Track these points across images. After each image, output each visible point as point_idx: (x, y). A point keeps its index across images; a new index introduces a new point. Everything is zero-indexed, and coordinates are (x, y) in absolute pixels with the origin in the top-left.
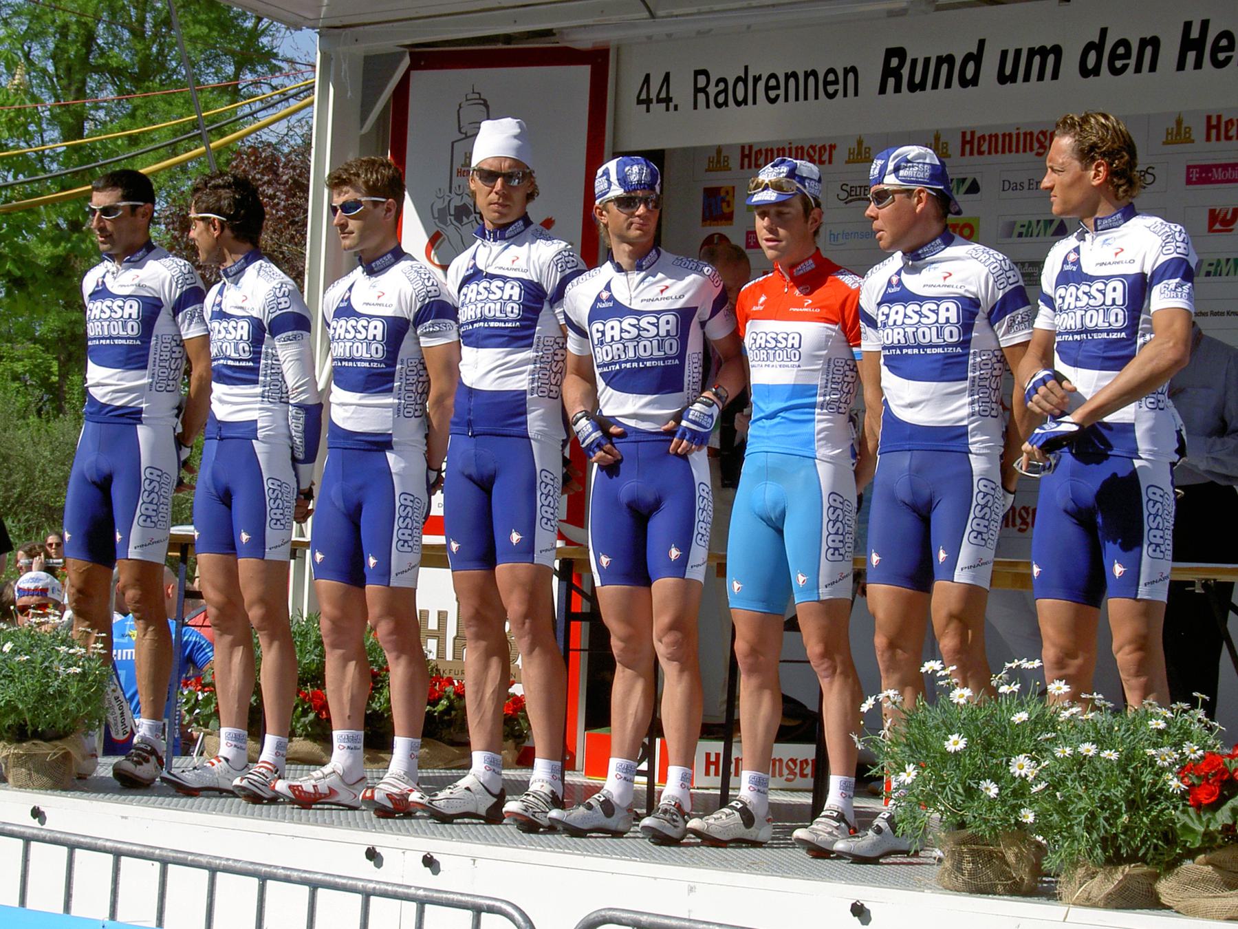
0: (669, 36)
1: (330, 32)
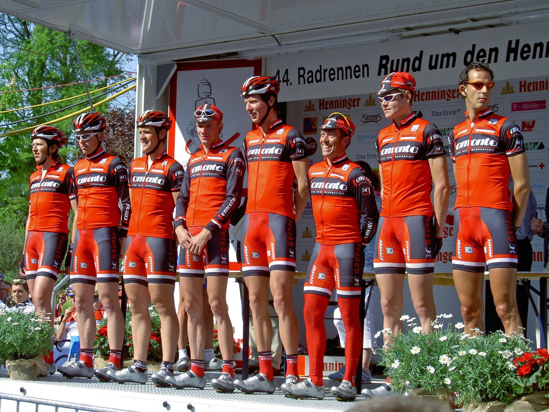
0: (287, 53)
1: (142, 55)
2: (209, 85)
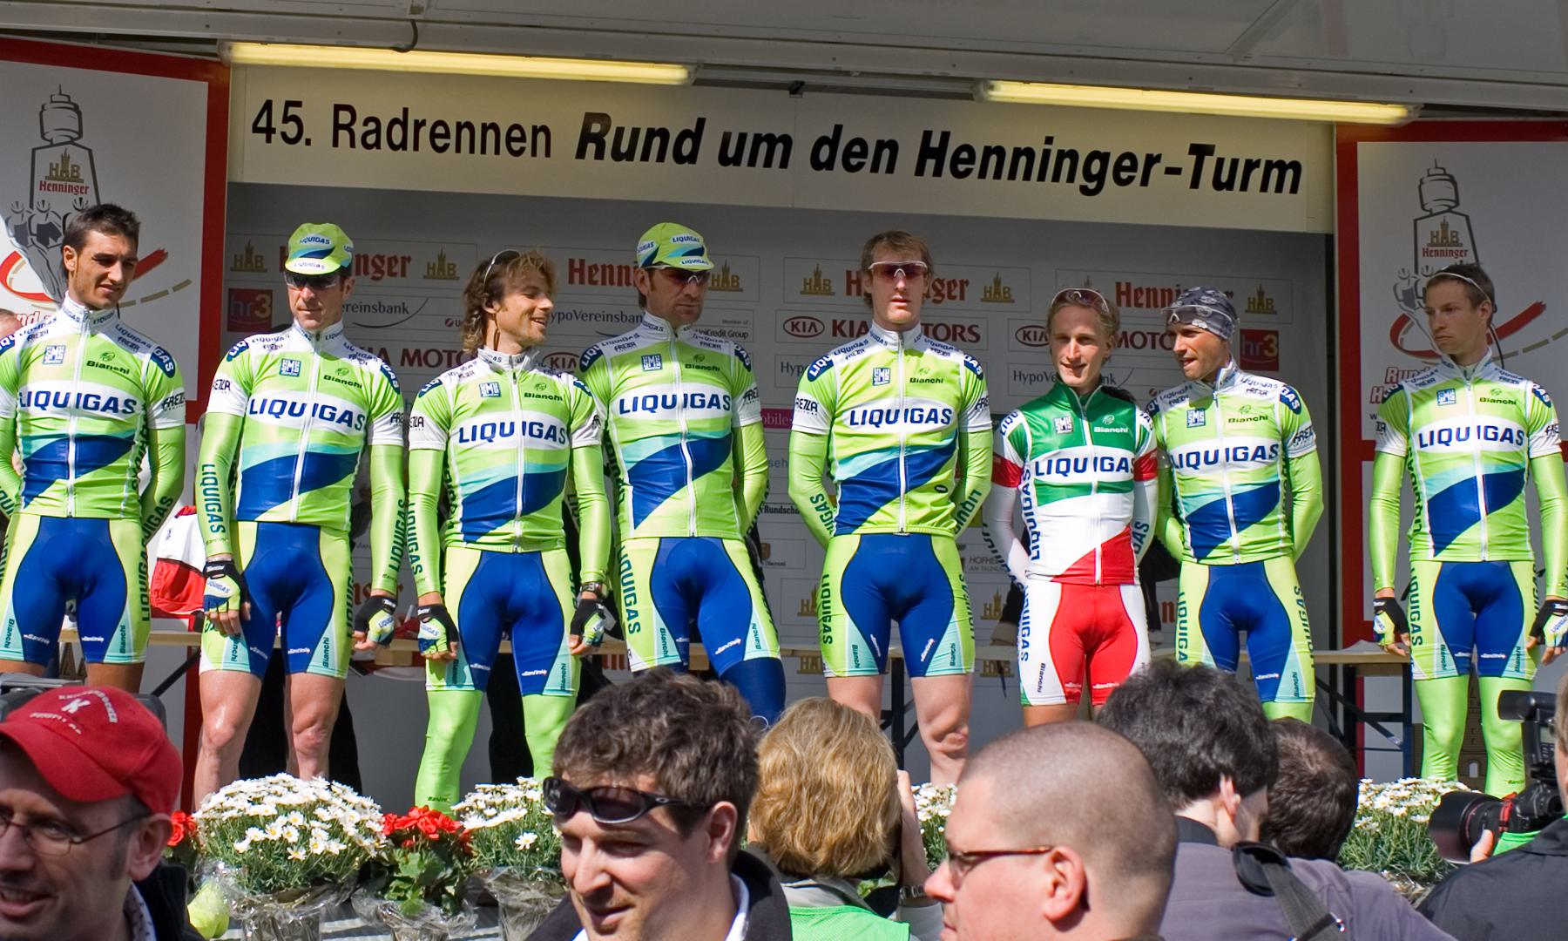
2: (76, 109)
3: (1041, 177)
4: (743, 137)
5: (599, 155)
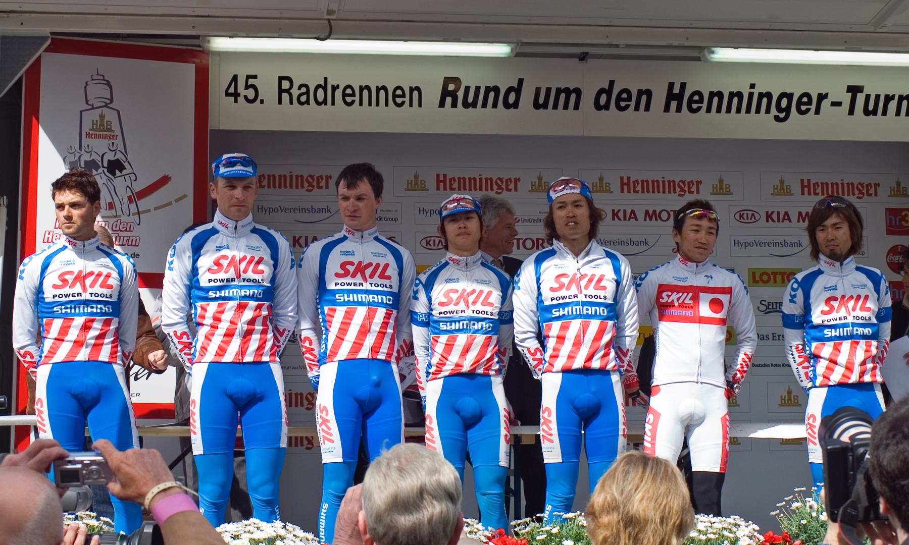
2: (108, 84)
3: (748, 111)
4: (549, 90)
5: (454, 105)
